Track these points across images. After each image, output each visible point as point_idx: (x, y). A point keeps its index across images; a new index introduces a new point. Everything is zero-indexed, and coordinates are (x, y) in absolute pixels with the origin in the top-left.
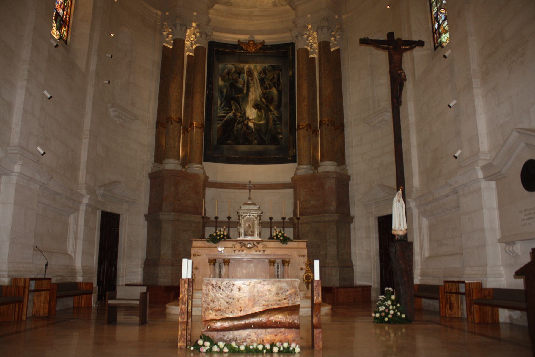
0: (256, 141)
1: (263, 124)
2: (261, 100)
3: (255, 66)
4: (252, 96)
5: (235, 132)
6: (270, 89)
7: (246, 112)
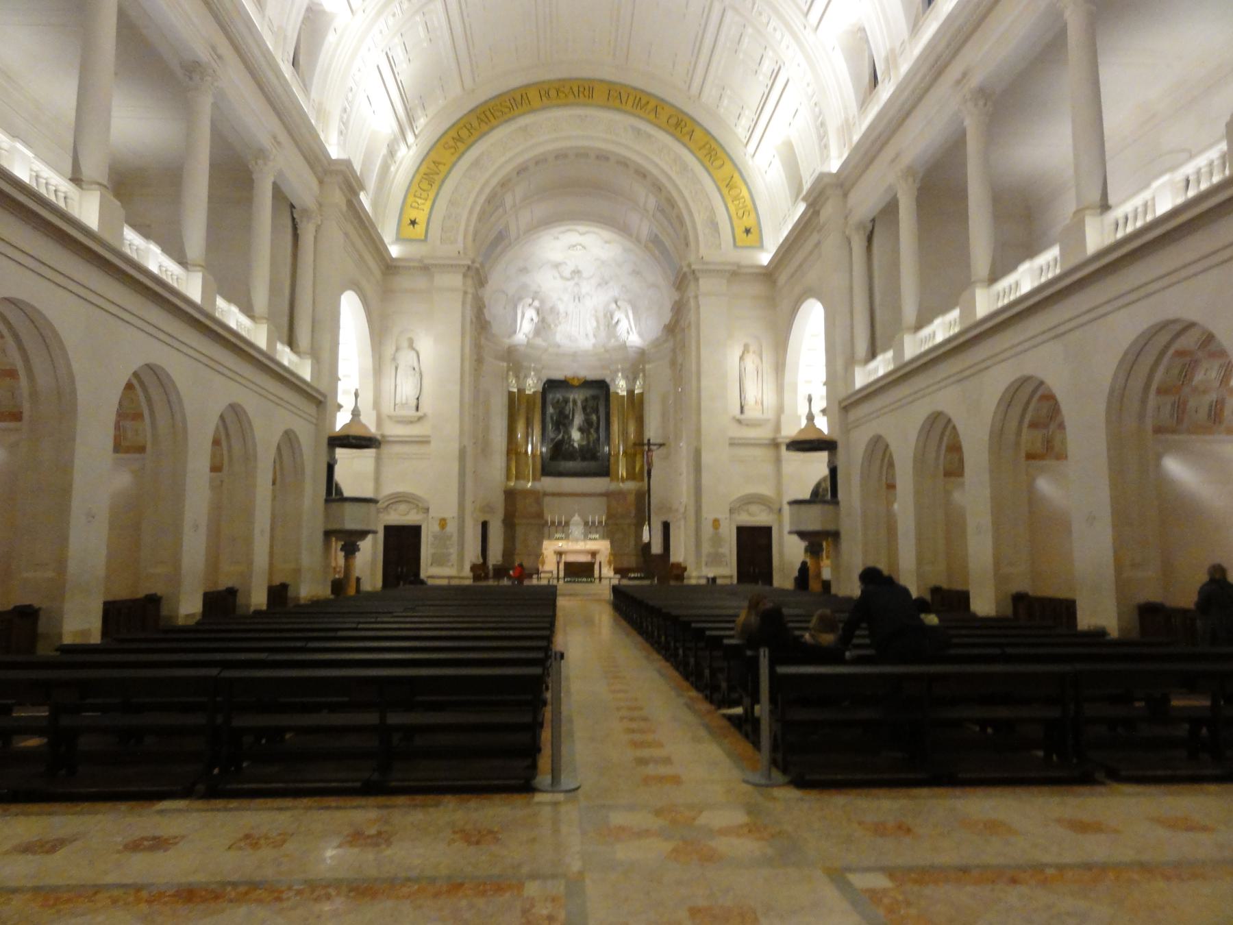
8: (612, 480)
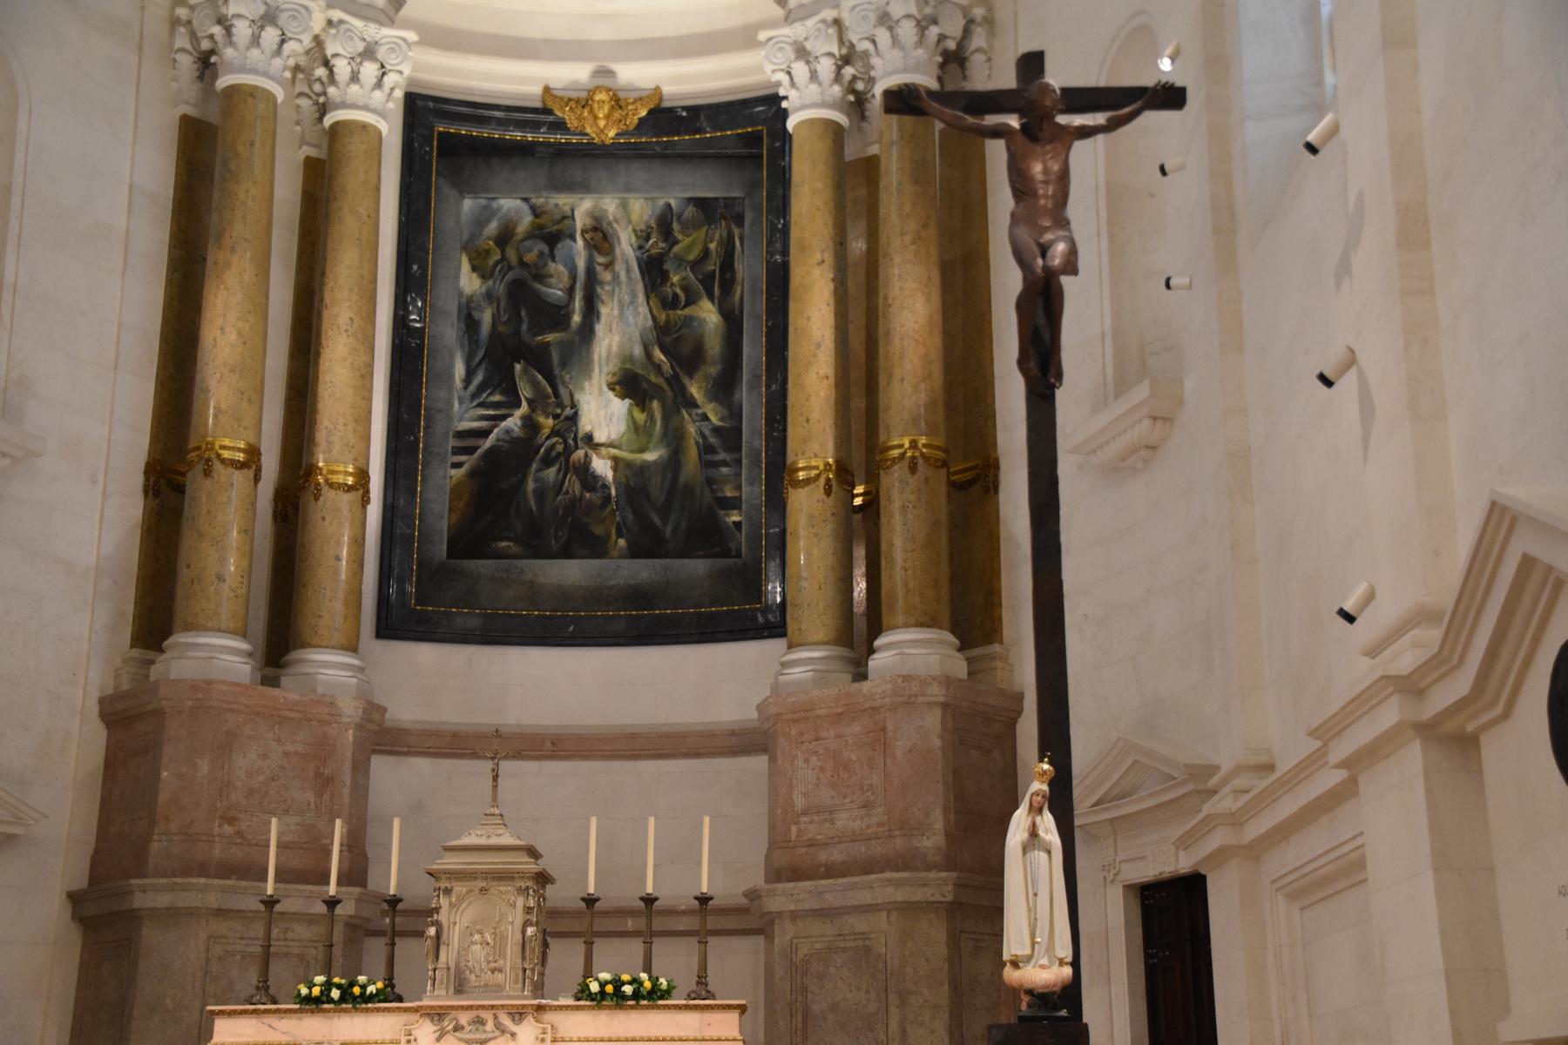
0: (622, 542)
1: (655, 462)
2: (648, 355)
3: (624, 205)
4: (607, 341)
5: (532, 503)
6: (685, 307)
7: (580, 413)
8: (791, 646)
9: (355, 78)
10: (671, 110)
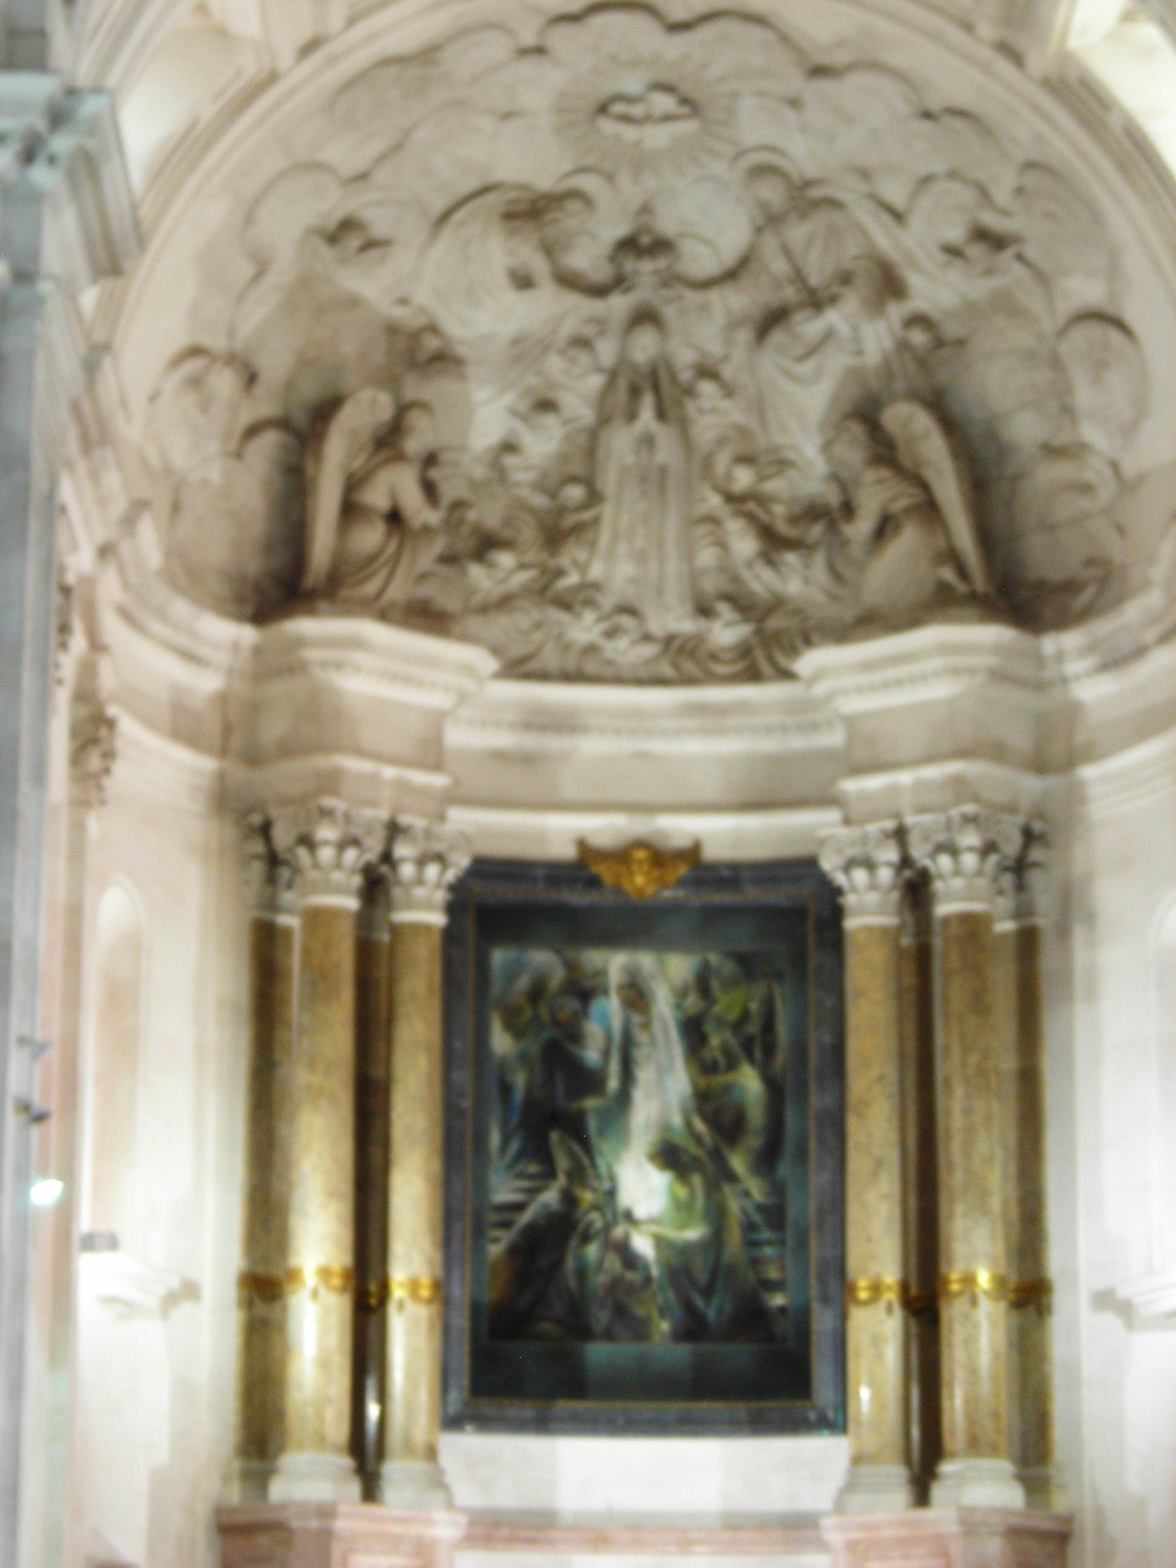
2: (689, 1125)
9: (420, 881)
10: (714, 867)
